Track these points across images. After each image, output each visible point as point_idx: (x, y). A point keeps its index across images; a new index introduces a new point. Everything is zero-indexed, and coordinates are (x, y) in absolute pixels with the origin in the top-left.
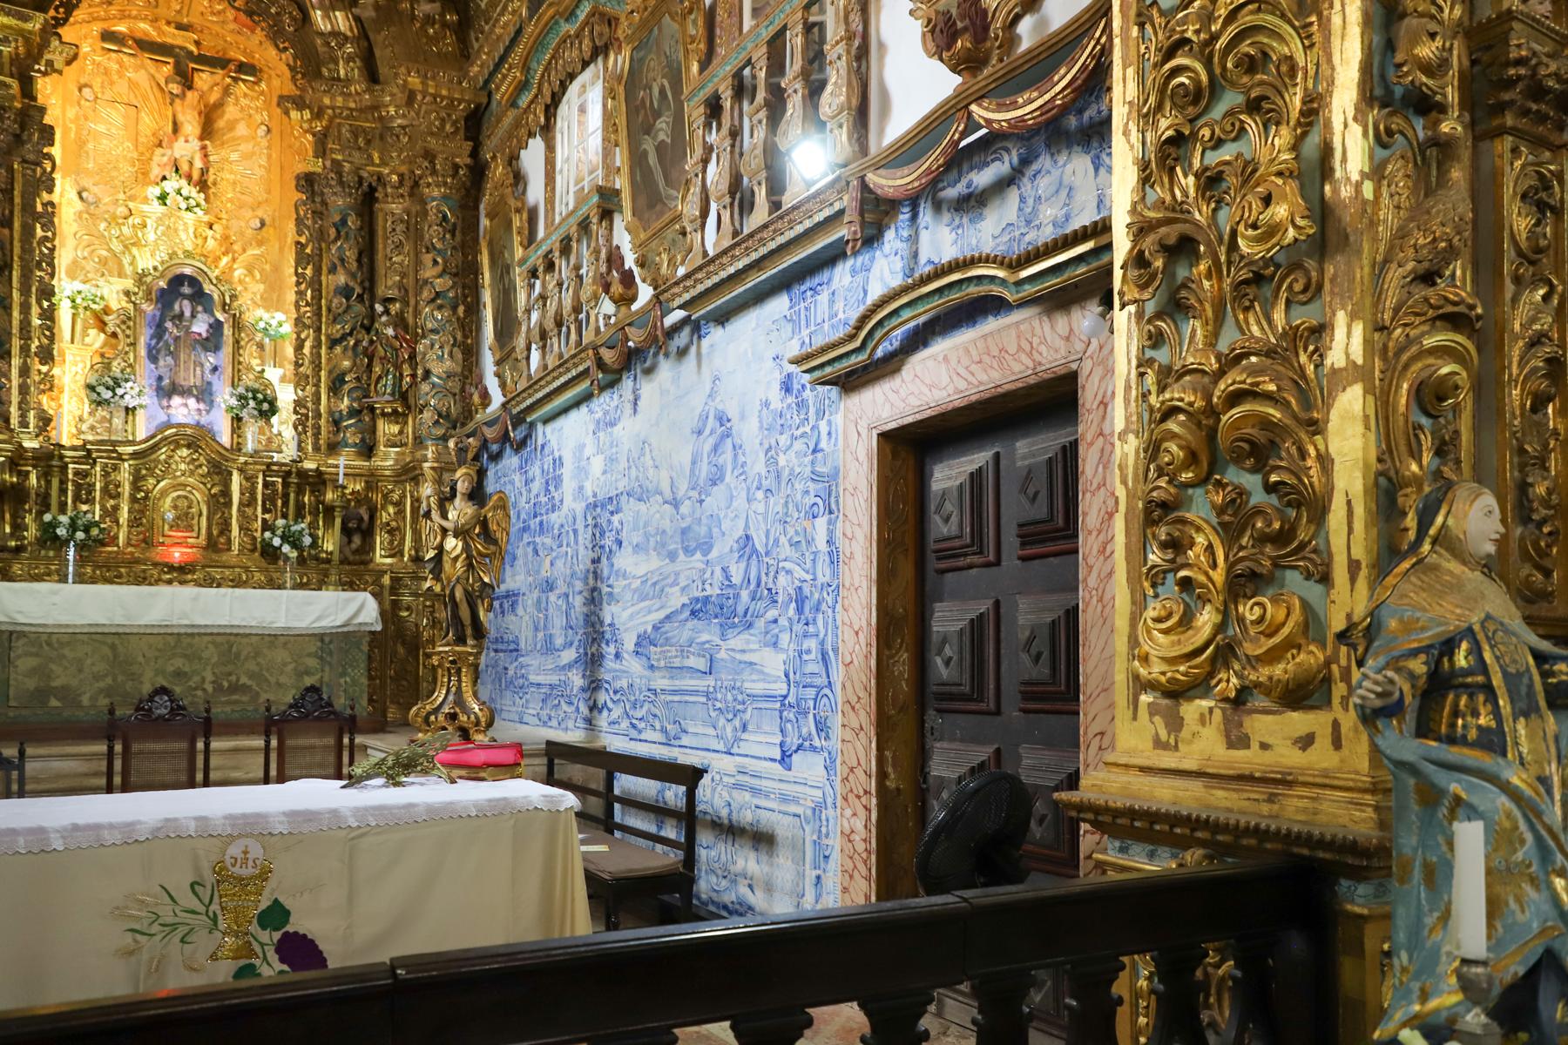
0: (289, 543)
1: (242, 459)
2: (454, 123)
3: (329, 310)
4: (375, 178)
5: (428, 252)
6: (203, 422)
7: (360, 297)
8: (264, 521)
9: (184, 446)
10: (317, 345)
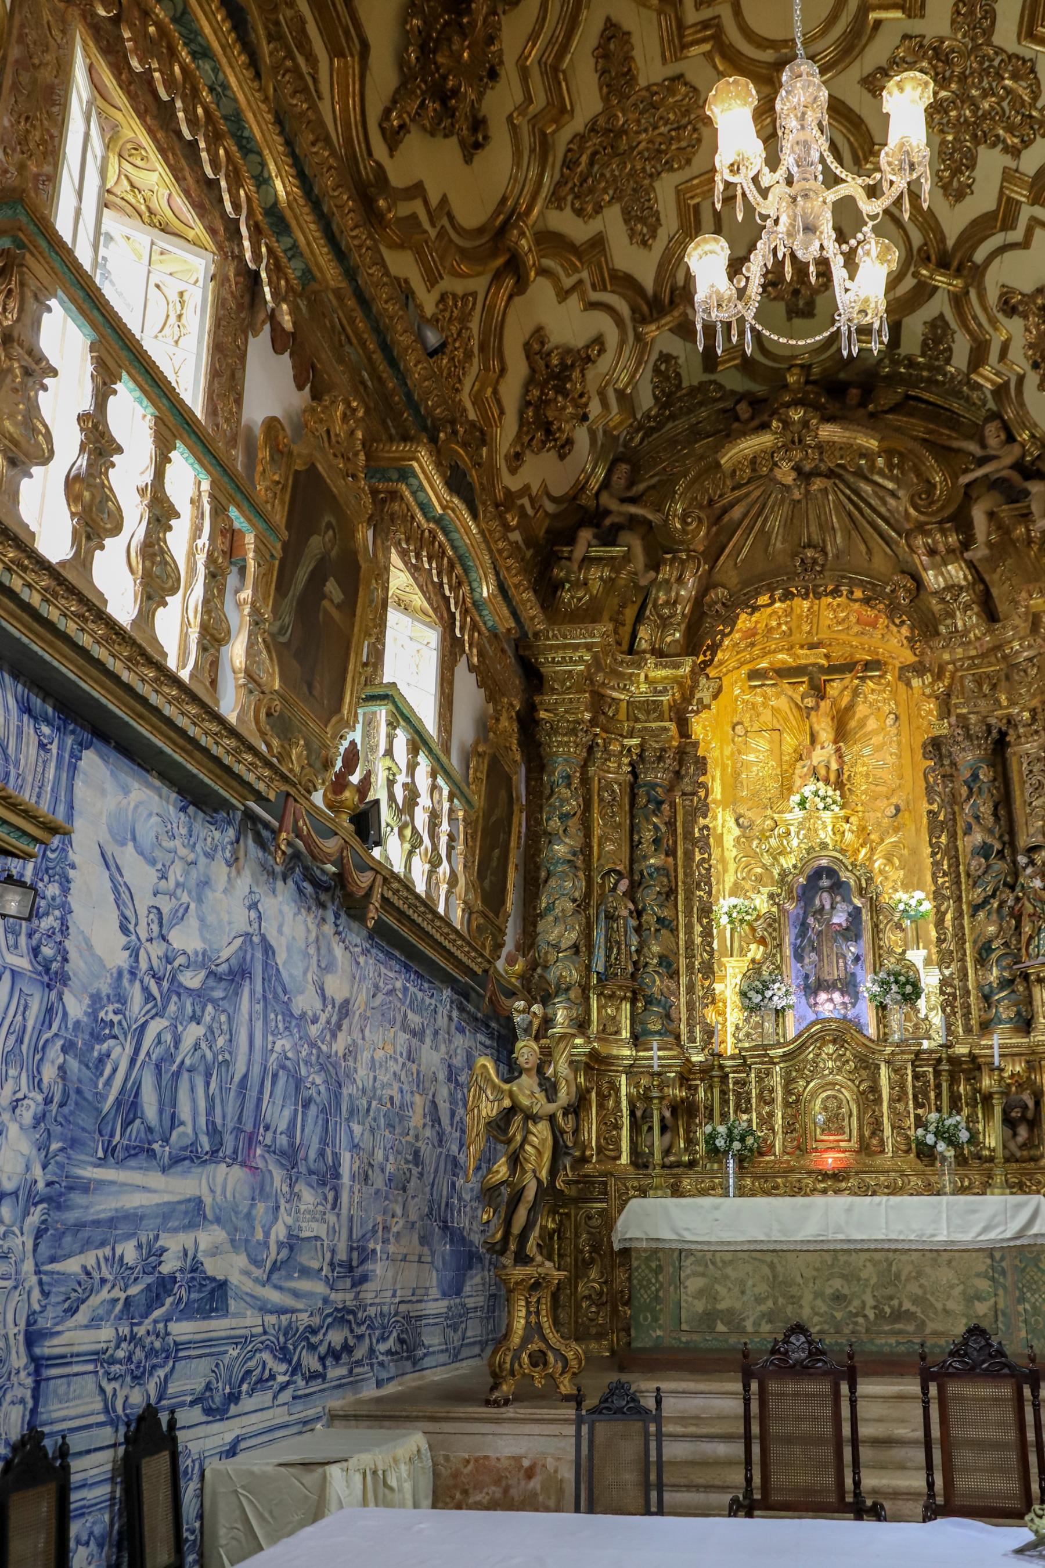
4: (1004, 721)
6: (850, 1014)
8: (918, 1117)
9: (830, 1041)
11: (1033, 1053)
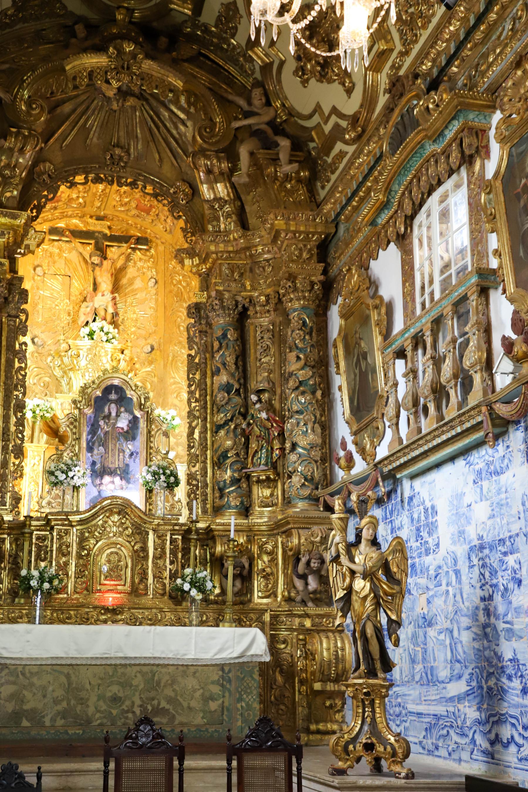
0: (195, 587)
1: (156, 522)
2: (310, 251)
3: (213, 403)
4: (248, 300)
5: (290, 352)
7: (238, 391)
10: (204, 432)
11: (251, 530)
